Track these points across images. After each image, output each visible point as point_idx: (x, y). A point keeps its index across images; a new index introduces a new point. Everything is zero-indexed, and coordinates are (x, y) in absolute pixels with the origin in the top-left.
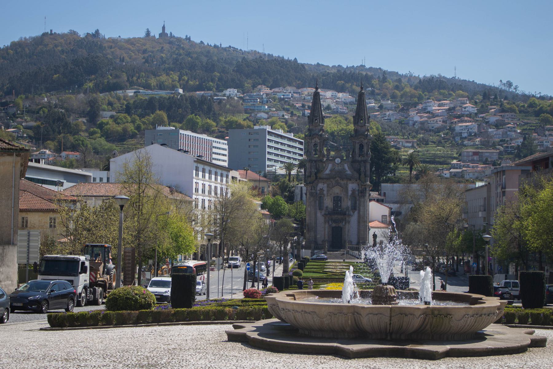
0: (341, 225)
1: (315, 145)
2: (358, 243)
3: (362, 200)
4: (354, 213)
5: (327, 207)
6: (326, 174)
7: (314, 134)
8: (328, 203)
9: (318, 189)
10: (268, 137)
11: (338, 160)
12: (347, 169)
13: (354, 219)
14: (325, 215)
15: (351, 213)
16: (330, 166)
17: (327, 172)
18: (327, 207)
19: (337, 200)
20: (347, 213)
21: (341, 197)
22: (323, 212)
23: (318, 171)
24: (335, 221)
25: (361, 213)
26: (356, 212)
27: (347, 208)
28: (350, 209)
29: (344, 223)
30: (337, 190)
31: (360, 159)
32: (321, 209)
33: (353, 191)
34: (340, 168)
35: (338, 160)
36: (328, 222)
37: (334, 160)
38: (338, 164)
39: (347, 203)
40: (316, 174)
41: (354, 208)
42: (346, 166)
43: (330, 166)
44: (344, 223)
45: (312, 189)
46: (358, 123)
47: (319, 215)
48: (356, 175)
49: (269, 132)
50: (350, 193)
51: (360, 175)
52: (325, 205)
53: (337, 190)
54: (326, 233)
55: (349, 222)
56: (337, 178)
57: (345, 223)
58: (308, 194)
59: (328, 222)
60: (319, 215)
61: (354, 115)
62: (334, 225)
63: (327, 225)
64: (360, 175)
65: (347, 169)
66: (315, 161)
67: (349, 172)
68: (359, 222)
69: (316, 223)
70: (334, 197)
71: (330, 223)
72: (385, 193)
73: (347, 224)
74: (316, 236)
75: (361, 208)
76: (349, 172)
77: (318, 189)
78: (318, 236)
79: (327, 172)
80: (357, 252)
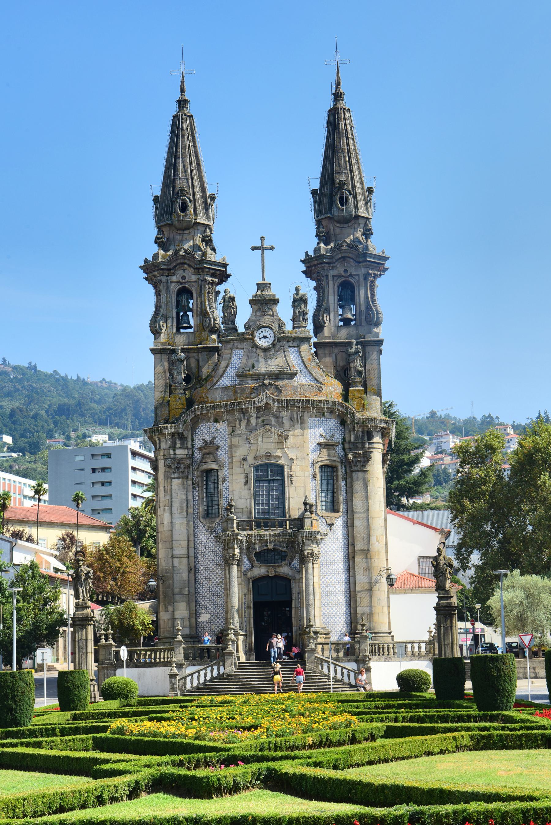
1: (184, 292)
3: (360, 474)
4: (330, 525)
6: (226, 388)
9: (198, 443)
10: (132, 462)
11: (263, 339)
16: (237, 358)
17: (229, 379)
21: (282, 467)
25: (357, 523)
27: (308, 507)
29: (296, 562)
34: (274, 364)
38: (266, 350)
44: (296, 562)
46: (330, 209)
49: (135, 454)
52: (224, 502)
58: (161, 463)
61: (317, 187)
62: (260, 571)
69: (193, 569)
71: (246, 564)
73: (310, 564)
74: (194, 615)
75: (358, 505)
77: (198, 443)
78: (204, 618)
79: (229, 379)
80: (352, 666)
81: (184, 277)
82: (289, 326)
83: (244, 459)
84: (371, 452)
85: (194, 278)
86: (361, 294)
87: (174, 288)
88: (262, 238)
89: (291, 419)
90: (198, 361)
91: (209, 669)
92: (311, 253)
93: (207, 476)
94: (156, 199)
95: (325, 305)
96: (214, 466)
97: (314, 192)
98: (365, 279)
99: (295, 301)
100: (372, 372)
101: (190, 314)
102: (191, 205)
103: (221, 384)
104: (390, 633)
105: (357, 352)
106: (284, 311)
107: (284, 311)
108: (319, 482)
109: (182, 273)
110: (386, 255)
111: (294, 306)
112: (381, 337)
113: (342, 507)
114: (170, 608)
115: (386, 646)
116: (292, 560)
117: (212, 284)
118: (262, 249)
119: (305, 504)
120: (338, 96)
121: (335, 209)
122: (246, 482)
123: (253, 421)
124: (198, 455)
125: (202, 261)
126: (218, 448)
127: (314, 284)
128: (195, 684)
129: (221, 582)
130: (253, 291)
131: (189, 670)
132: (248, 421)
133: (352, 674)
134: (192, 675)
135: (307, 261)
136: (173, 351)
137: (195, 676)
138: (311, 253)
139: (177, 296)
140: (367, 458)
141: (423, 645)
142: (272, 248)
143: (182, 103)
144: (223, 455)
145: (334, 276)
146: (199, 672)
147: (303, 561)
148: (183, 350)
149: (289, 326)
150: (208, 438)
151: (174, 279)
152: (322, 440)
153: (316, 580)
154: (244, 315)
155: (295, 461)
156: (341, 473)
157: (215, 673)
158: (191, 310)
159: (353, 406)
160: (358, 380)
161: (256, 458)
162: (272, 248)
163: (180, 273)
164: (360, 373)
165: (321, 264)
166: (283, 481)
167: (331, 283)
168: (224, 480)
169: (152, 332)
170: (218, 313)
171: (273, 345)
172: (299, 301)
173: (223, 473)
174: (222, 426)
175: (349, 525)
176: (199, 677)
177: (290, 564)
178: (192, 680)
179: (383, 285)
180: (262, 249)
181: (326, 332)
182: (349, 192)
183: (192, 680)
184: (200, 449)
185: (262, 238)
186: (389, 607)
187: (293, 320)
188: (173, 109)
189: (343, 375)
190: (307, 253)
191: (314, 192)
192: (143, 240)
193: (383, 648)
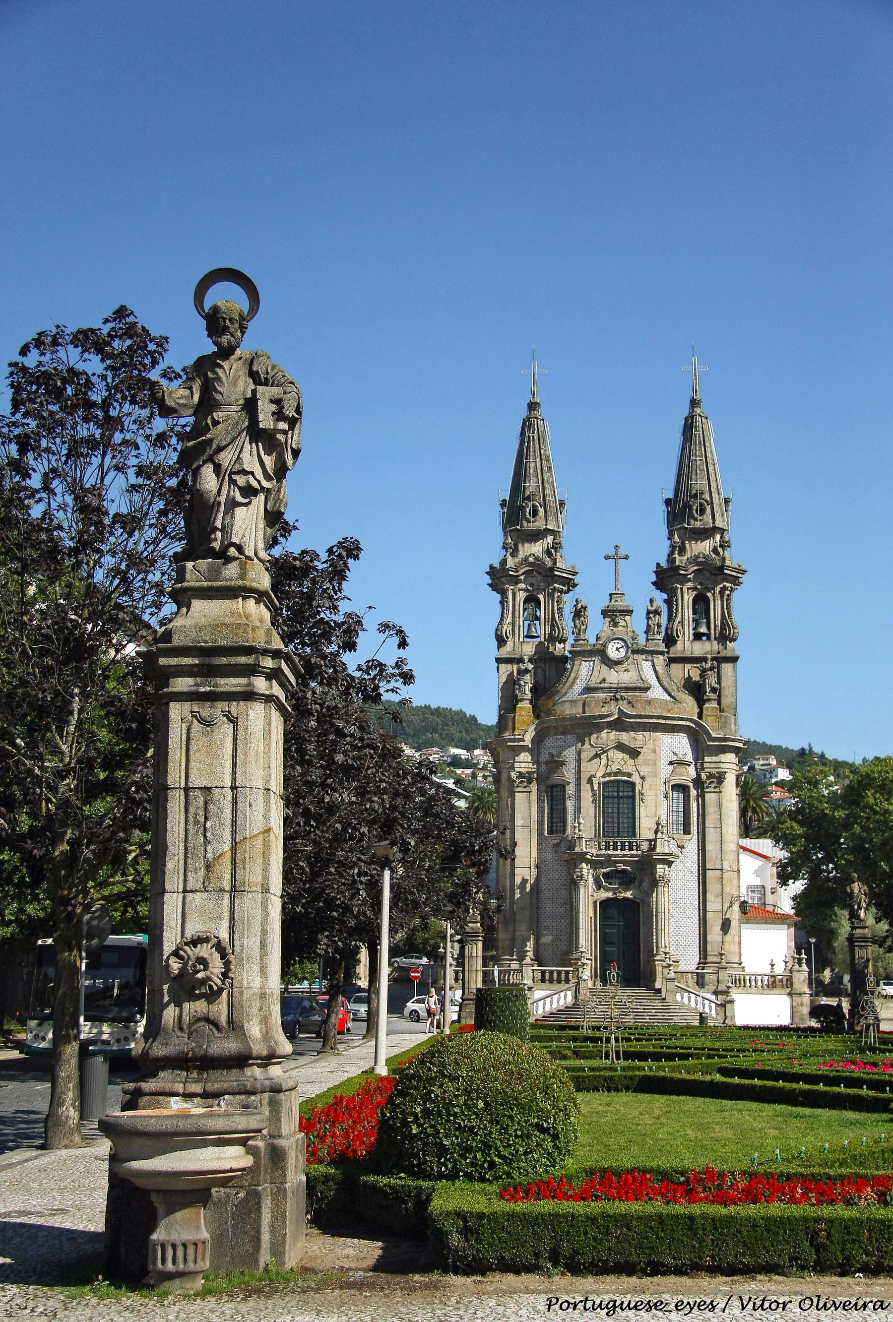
21: (633, 785)
29: (646, 884)
37: (605, 646)
39: (654, 810)
42: (647, 667)
50: (666, 771)
61: (671, 495)
82: (642, 639)
84: (725, 773)
86: (716, 610)
88: (617, 547)
90: (545, 671)
91: (562, 994)
92: (664, 564)
93: (552, 792)
94: (503, 504)
95: (679, 619)
97: (668, 502)
98: (722, 593)
99: (649, 612)
100: (727, 689)
102: (541, 511)
103: (570, 696)
104: (740, 964)
105: (712, 669)
107: (637, 623)
109: (532, 579)
110: (743, 568)
111: (648, 618)
112: (737, 653)
114: (511, 929)
115: (748, 977)
116: (641, 881)
117: (561, 592)
119: (658, 824)
120: (694, 403)
125: (552, 569)
127: (665, 596)
129: (565, 903)
130: (604, 603)
131: (538, 994)
133: (713, 1005)
135: (659, 571)
136: (520, 660)
137: (548, 1000)
138: (664, 564)
139: (524, 604)
140: (720, 778)
141: (766, 978)
142: (626, 558)
143: (532, 406)
145: (688, 589)
147: (654, 883)
148: (530, 660)
152: (674, 758)
154: (596, 626)
155: (647, 779)
156: (691, 793)
159: (709, 724)
160: (713, 696)
162: (626, 558)
164: (714, 690)
165: (675, 575)
166: (633, 797)
167: (686, 597)
169: (497, 639)
170: (567, 623)
173: (570, 790)
176: (552, 1002)
177: (639, 886)
178: (544, 1005)
179: (739, 598)
181: (679, 646)
182: (707, 501)
183: (544, 1005)
185: (617, 547)
186: (740, 936)
187: (647, 632)
188: (524, 413)
189: (696, 690)
190: (658, 565)
191: (668, 502)
192: (491, 546)
193: (740, 980)
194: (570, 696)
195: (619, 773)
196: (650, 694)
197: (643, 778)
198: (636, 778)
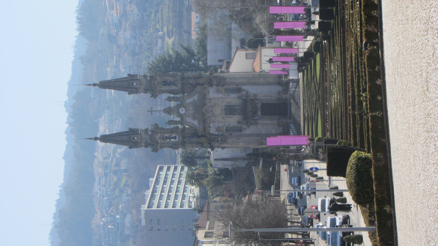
0: (259, 105)
2: (280, 83)
3: (228, 80)
4: (244, 90)
5: (239, 122)
6: (199, 124)
7: (151, 140)
8: (233, 120)
9: (216, 133)
10: (155, 208)
11: (182, 111)
12: (191, 100)
13: (252, 90)
14: (248, 124)
15: (244, 93)
17: (196, 123)
18: (239, 122)
19: (230, 110)
20: (244, 98)
21: (226, 106)
22: (245, 127)
23: (195, 134)
24: (255, 113)
25: (244, 82)
26: (244, 87)
27: (239, 98)
28: (239, 94)
29: (257, 102)
30: (218, 111)
31: (180, 85)
32: (240, 130)
33: (218, 91)
34: (191, 108)
35: (182, 111)
36: (257, 120)
37: (181, 115)
38: (186, 110)
39: (233, 99)
40: (199, 137)
41: (239, 90)
43: (189, 120)
44: (257, 102)
45: (218, 141)
47: (248, 131)
48: (198, 89)
49: (149, 207)
50: (220, 95)
51: (198, 84)
53: (218, 111)
54: (269, 122)
55: (255, 95)
56: (204, 111)
57: (257, 99)
58: (223, 146)
59: (257, 120)
60: (248, 131)
61: (127, 93)
62: (259, 113)
63: (260, 122)
64: (198, 84)
65: (191, 100)
66: (184, 137)
67: (196, 97)
68: (255, 84)
70: (226, 114)
71: (257, 118)
72: (219, 61)
73: (258, 97)
76: (196, 97)
79: (196, 123)
80: (291, 84)
81: (160, 138)
83: (223, 118)
85: (159, 135)
87: (163, 141)
88: (148, 111)
89: (210, 102)
96: (225, 128)
101: (171, 136)
103: (197, 126)
106: (173, 104)
107: (173, 104)
108: (231, 94)
113: (239, 86)
118: (152, 111)
121: (137, 87)
122: (231, 117)
123: (211, 115)
124: (220, 133)
126: (218, 127)
128: (295, 131)
132: (211, 116)
134: (293, 133)
144: (221, 125)
146: (292, 131)
149: (179, 103)
150: (215, 130)
151: (159, 141)
153: (262, 95)
157: (293, 125)
158: (170, 136)
161: (222, 114)
162: (152, 108)
163: (157, 139)
167: (163, 89)
168: (229, 125)
171: (185, 108)
172: (169, 99)
174: (211, 125)
175: (244, 84)
180: (152, 111)
184: (218, 132)
185: (148, 111)
191: (129, 94)
194: (197, 126)
195: (222, 110)
196: (196, 100)
197: (223, 102)
198: (224, 104)
